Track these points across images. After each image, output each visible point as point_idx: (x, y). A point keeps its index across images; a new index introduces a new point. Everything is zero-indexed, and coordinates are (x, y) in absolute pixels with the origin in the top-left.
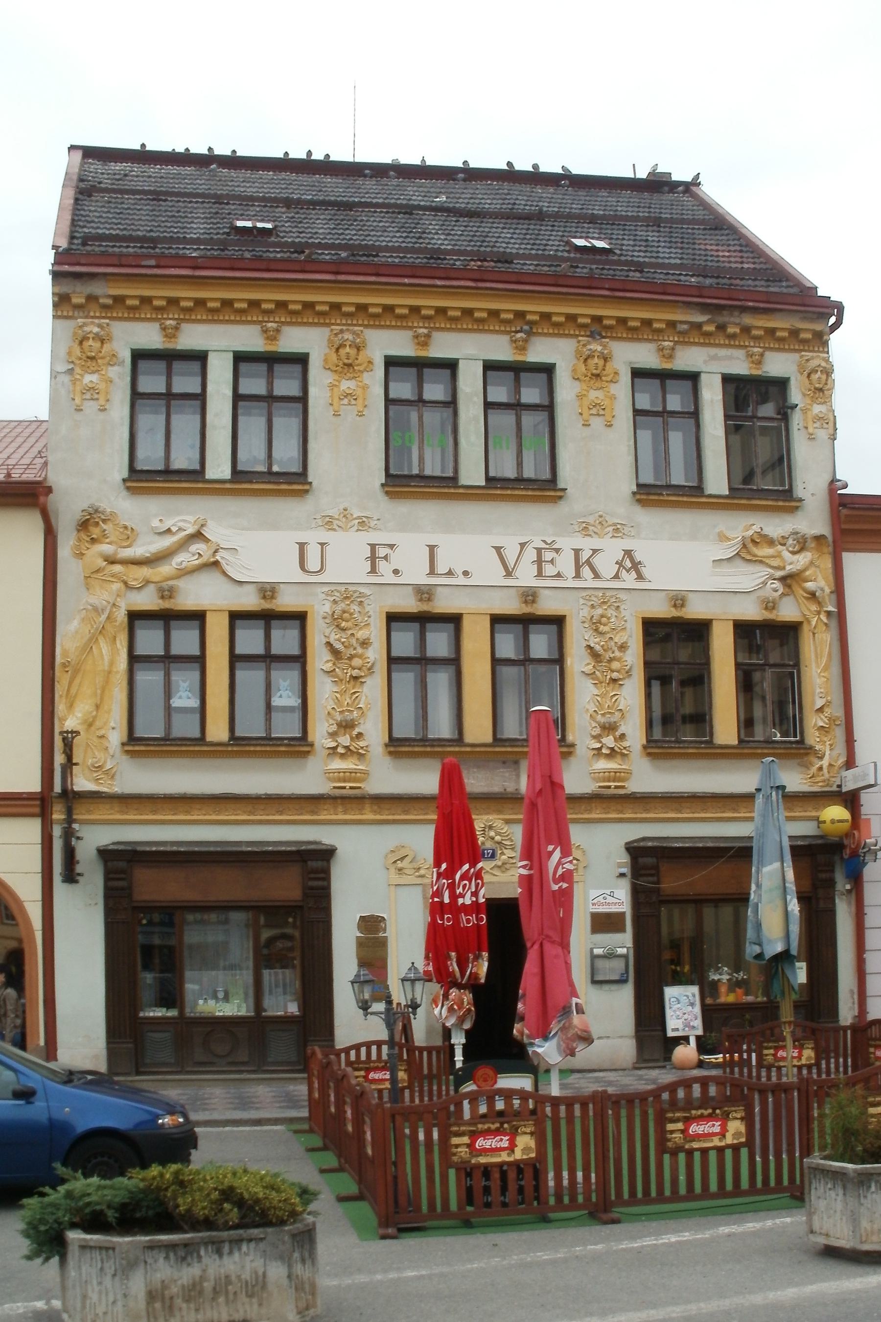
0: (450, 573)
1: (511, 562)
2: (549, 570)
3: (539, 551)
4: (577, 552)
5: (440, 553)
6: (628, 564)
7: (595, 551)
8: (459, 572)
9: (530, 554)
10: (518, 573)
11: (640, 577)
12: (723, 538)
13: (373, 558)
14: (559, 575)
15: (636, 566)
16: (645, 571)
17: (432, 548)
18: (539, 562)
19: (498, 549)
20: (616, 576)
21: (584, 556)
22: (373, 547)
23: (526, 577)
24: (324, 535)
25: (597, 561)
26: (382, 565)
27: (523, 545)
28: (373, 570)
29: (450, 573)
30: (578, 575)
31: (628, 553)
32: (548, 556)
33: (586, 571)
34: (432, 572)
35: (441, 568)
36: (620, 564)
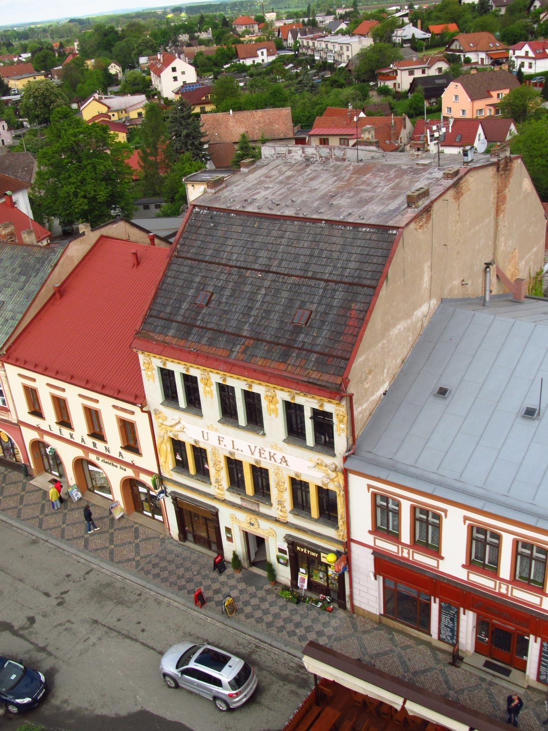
0: (238, 449)
1: (253, 450)
2: (262, 455)
3: (260, 450)
4: (270, 453)
5: (235, 443)
6: (284, 460)
7: (275, 454)
8: (240, 450)
9: (257, 450)
10: (255, 454)
11: (287, 465)
12: (310, 460)
13: (219, 440)
14: (265, 458)
15: (286, 461)
16: (288, 464)
17: (233, 441)
18: (260, 453)
19: (249, 446)
20: (281, 463)
21: (272, 455)
22: (219, 437)
23: (257, 456)
24: (208, 431)
25: (275, 456)
26: (221, 442)
27: (255, 447)
28: (220, 443)
29: (238, 449)
30: (270, 459)
31: (284, 457)
32: (262, 452)
33: (272, 459)
34: (233, 448)
35: (236, 447)
36: (281, 459)
